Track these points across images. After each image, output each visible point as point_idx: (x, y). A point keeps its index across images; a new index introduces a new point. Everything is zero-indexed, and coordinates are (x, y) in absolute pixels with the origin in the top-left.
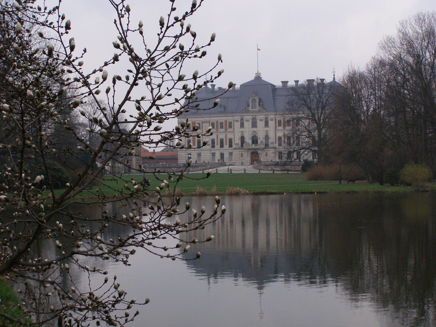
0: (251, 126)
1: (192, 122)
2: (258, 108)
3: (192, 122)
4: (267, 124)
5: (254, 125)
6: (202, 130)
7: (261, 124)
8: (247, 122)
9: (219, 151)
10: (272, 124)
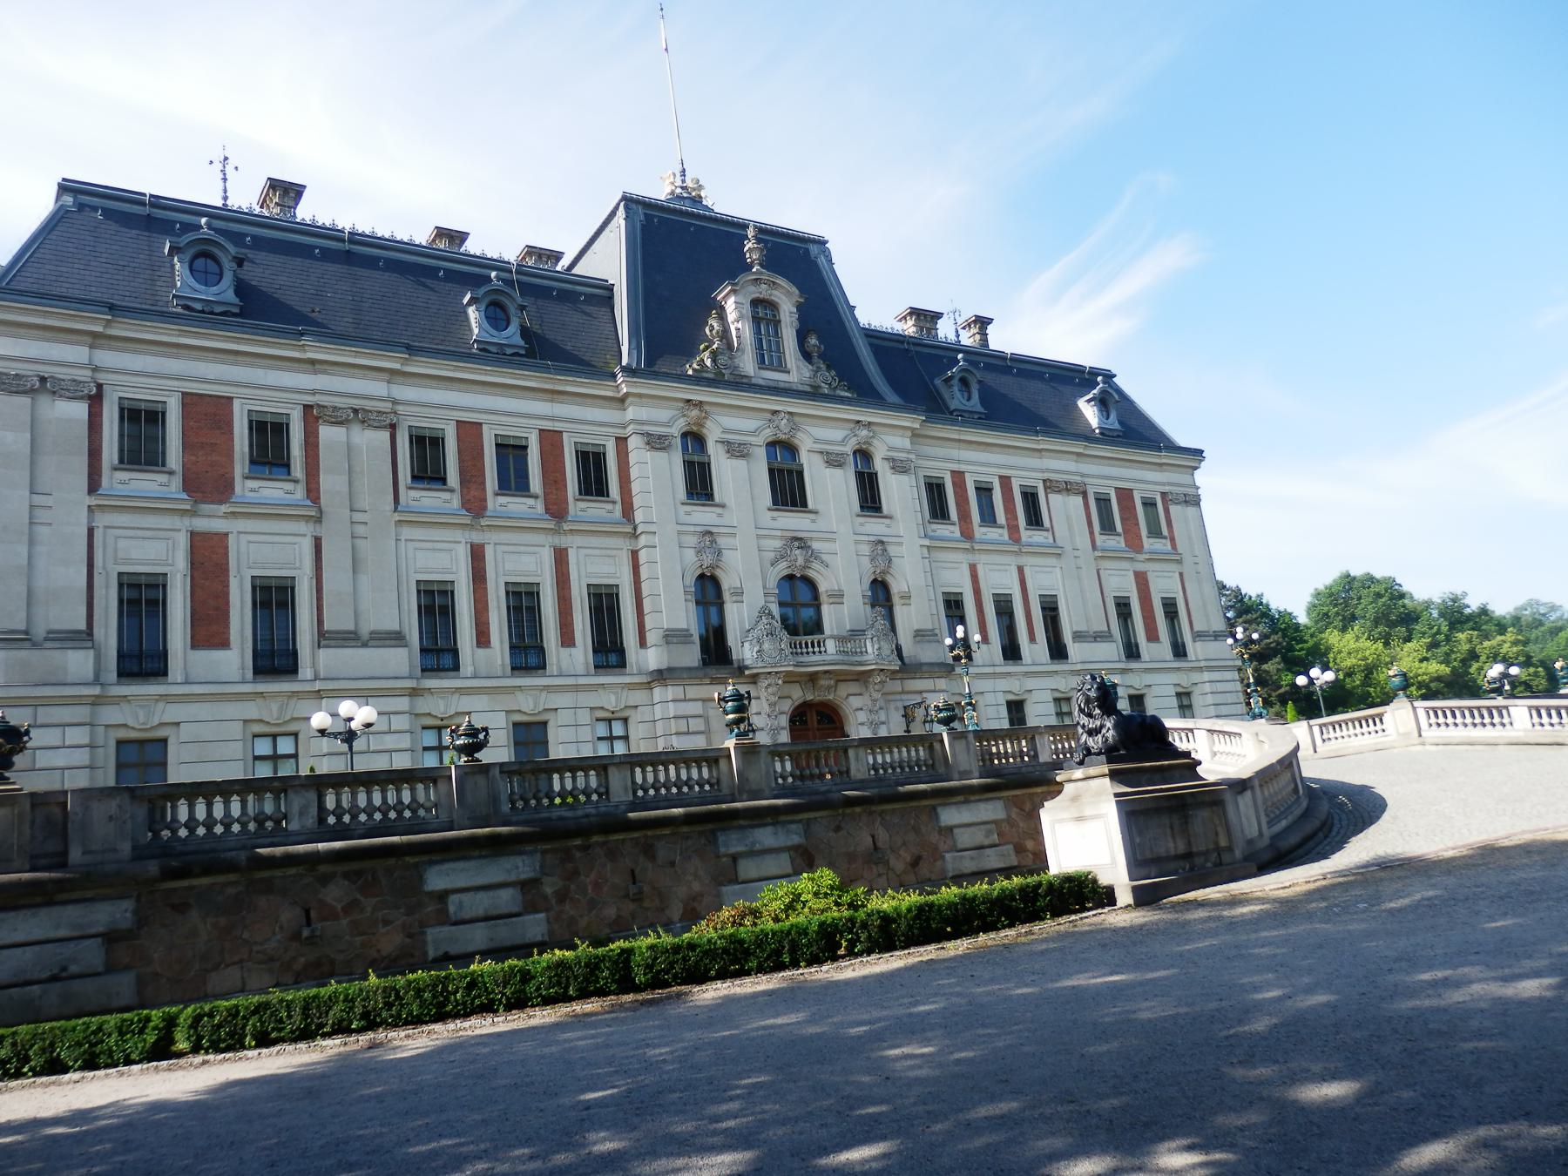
0: (768, 501)
1: (190, 401)
2: (797, 372)
3: (190, 401)
4: (870, 498)
5: (788, 489)
6: (313, 492)
7: (830, 488)
8: (741, 464)
9: (509, 702)
10: (899, 492)
